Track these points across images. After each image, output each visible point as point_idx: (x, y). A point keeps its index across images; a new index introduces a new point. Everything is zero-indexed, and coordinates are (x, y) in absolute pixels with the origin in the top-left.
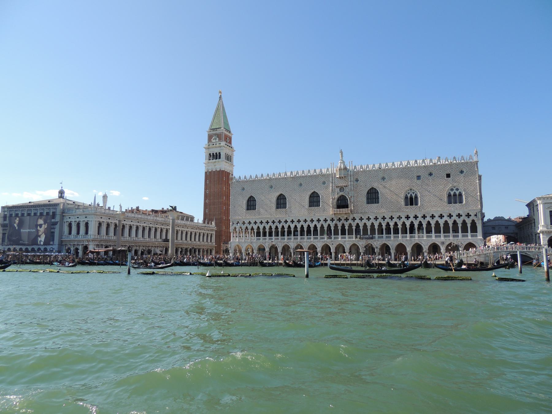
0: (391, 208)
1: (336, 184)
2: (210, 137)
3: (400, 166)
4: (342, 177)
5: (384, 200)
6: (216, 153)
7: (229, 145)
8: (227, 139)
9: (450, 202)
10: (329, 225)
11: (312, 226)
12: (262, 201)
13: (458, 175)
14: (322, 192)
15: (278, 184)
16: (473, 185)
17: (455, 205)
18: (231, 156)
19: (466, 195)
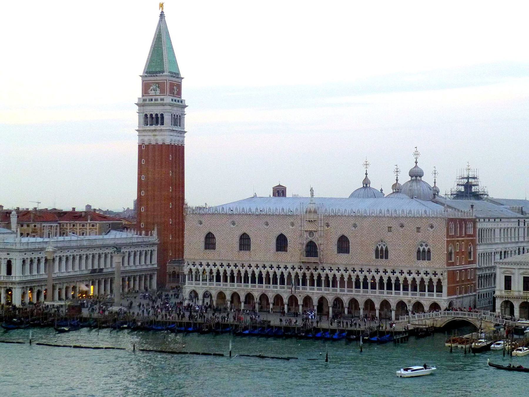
0: (361, 261)
1: (306, 227)
2: (146, 87)
5: (354, 251)
6: (157, 115)
7: (177, 99)
8: (173, 89)
9: (418, 259)
10: (297, 273)
12: (223, 240)
14: (290, 235)
15: (242, 221)
18: (180, 116)
19: (434, 253)
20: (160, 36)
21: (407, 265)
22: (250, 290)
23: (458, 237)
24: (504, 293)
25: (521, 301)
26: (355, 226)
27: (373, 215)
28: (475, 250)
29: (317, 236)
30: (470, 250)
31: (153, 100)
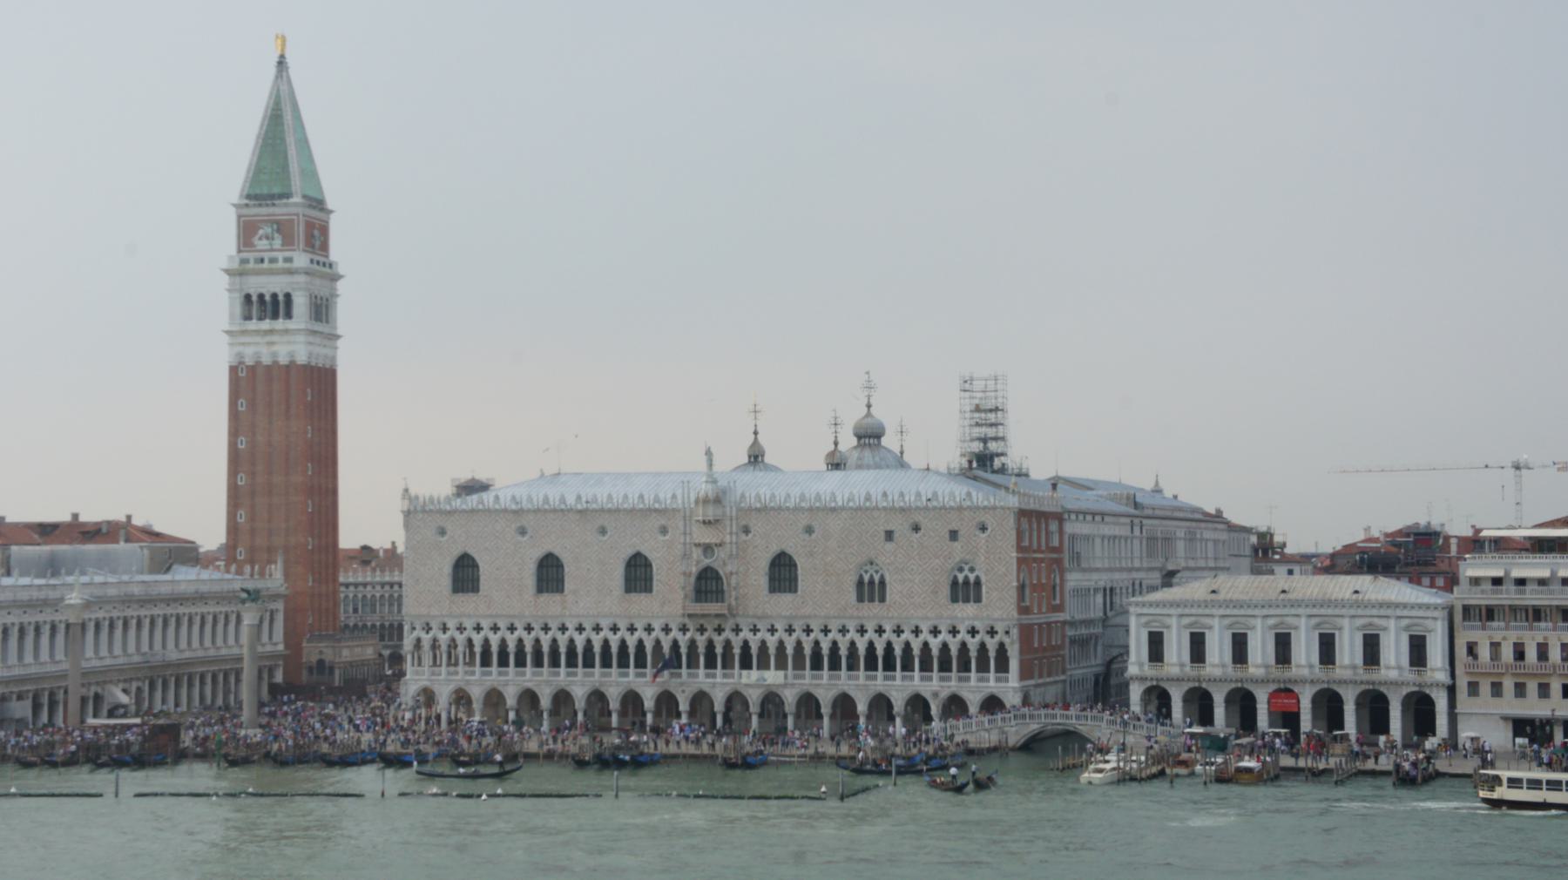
1: (695, 536)
2: (247, 232)
3: (847, 503)
4: (710, 522)
6: (274, 296)
7: (322, 259)
8: (313, 236)
9: (954, 599)
11: (631, 642)
12: (497, 569)
13: (975, 535)
14: (659, 555)
16: (1004, 562)
17: (965, 608)
20: (279, 112)
21: (929, 615)
22: (563, 684)
23: (1035, 552)
24: (1149, 670)
25: (1186, 687)
26: (809, 530)
27: (851, 504)
28: (1062, 580)
29: (723, 556)
30: (1054, 580)
31: (266, 261)
